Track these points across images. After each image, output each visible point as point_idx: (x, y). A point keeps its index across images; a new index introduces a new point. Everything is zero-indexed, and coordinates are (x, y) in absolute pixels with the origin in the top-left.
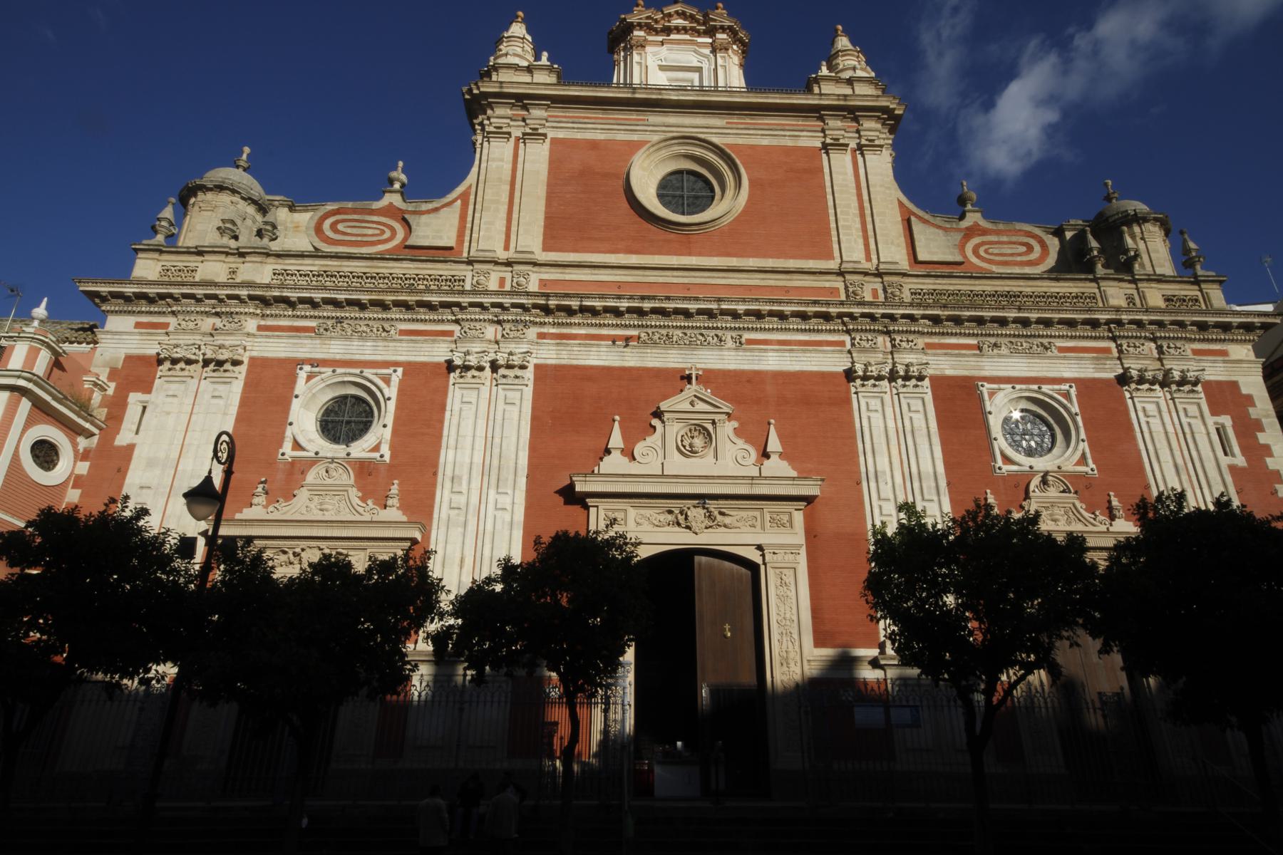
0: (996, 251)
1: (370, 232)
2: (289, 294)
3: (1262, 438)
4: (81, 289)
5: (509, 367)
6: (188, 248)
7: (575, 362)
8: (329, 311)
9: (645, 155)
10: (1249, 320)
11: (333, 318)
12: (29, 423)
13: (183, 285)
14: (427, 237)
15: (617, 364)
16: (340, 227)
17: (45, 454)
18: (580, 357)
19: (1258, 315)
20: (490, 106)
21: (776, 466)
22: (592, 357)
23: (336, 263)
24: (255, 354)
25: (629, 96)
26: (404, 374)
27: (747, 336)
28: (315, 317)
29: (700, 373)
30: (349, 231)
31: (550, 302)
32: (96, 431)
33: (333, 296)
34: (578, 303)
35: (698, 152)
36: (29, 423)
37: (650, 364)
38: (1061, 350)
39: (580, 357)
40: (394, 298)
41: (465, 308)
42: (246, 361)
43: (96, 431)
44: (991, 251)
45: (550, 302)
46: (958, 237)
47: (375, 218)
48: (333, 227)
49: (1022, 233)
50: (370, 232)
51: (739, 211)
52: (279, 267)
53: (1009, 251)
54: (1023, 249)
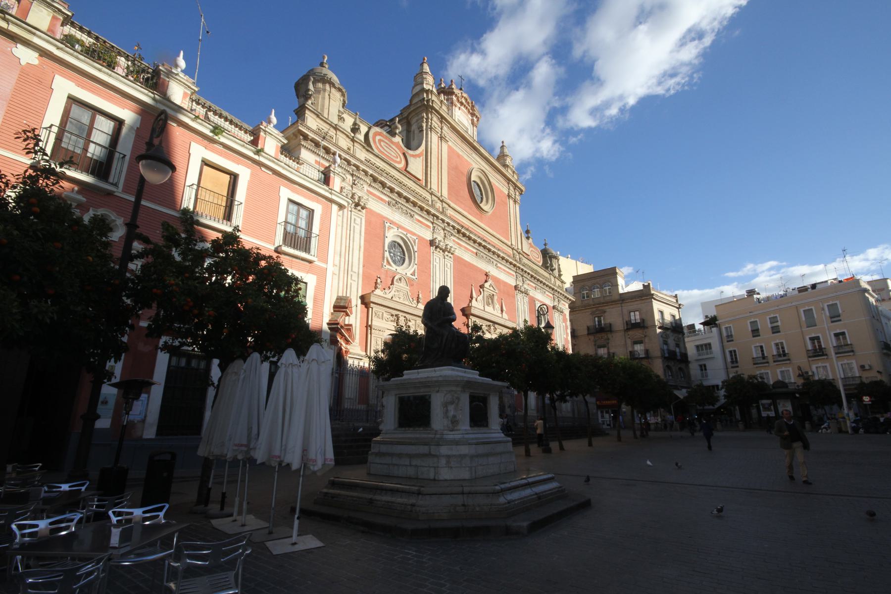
1: (393, 154)
2: (387, 182)
4: (300, 128)
5: (449, 252)
6: (332, 122)
7: (462, 257)
8: (395, 196)
11: (395, 200)
13: (348, 154)
14: (412, 169)
15: (472, 262)
16: (382, 144)
20: (431, 113)
21: (505, 316)
23: (388, 167)
25: (472, 142)
27: (499, 265)
28: (389, 196)
30: (385, 148)
33: (402, 192)
35: (483, 178)
37: (479, 266)
38: (547, 295)
41: (439, 219)
45: (462, 230)
47: (394, 147)
48: (380, 141)
50: (393, 154)
52: (368, 157)
54: (537, 256)
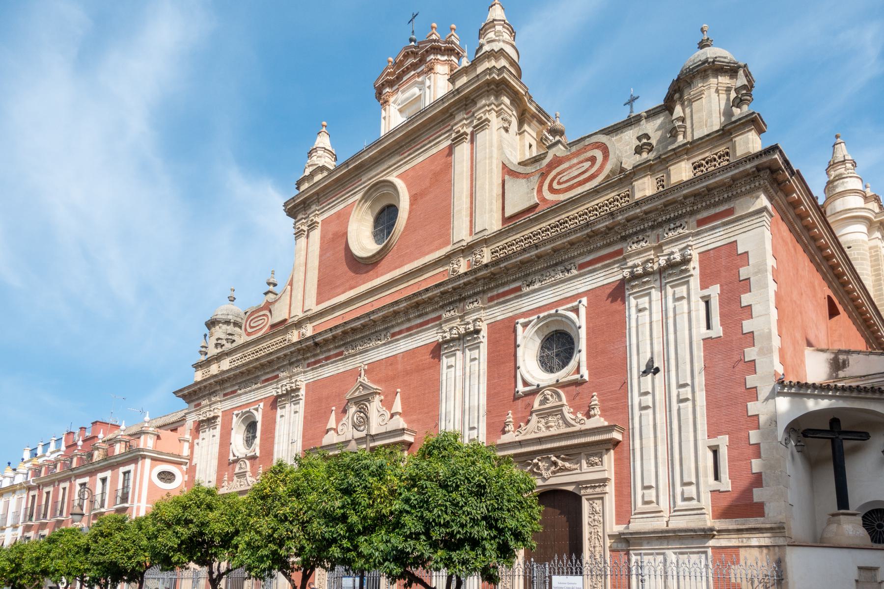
0: (565, 179)
3: (746, 299)
9: (357, 210)
10: (741, 169)
12: (152, 467)
17: (167, 477)
18: (321, 374)
19: (765, 153)
22: (401, 344)
24: (223, 410)
26: (264, 405)
29: (366, 367)
31: (303, 345)
32: (188, 461)
34: (312, 342)
36: (152, 467)
39: (321, 374)
40: (276, 356)
42: (220, 414)
43: (188, 461)
44: (561, 181)
46: (535, 179)
49: (590, 147)
51: (402, 230)
53: (576, 173)
